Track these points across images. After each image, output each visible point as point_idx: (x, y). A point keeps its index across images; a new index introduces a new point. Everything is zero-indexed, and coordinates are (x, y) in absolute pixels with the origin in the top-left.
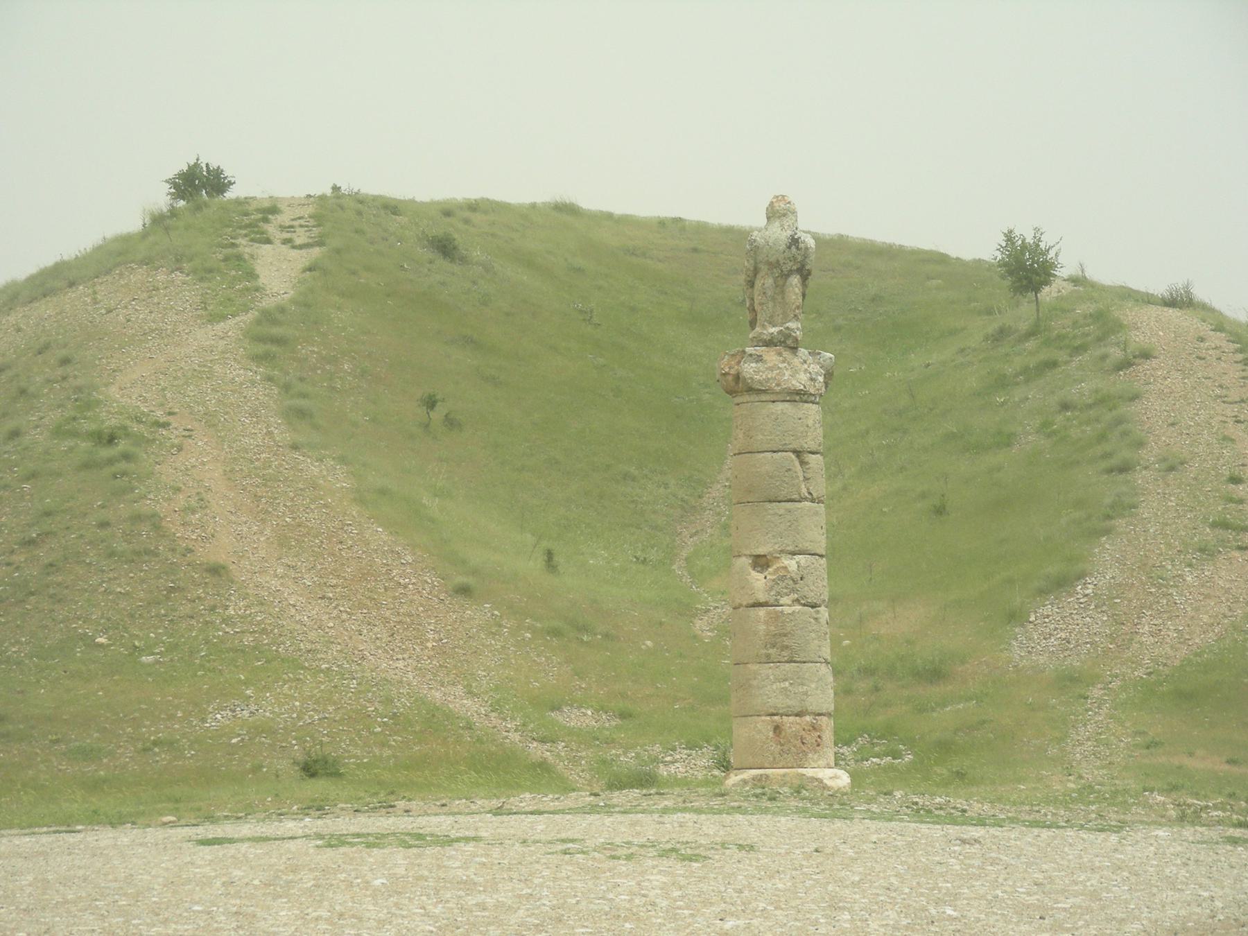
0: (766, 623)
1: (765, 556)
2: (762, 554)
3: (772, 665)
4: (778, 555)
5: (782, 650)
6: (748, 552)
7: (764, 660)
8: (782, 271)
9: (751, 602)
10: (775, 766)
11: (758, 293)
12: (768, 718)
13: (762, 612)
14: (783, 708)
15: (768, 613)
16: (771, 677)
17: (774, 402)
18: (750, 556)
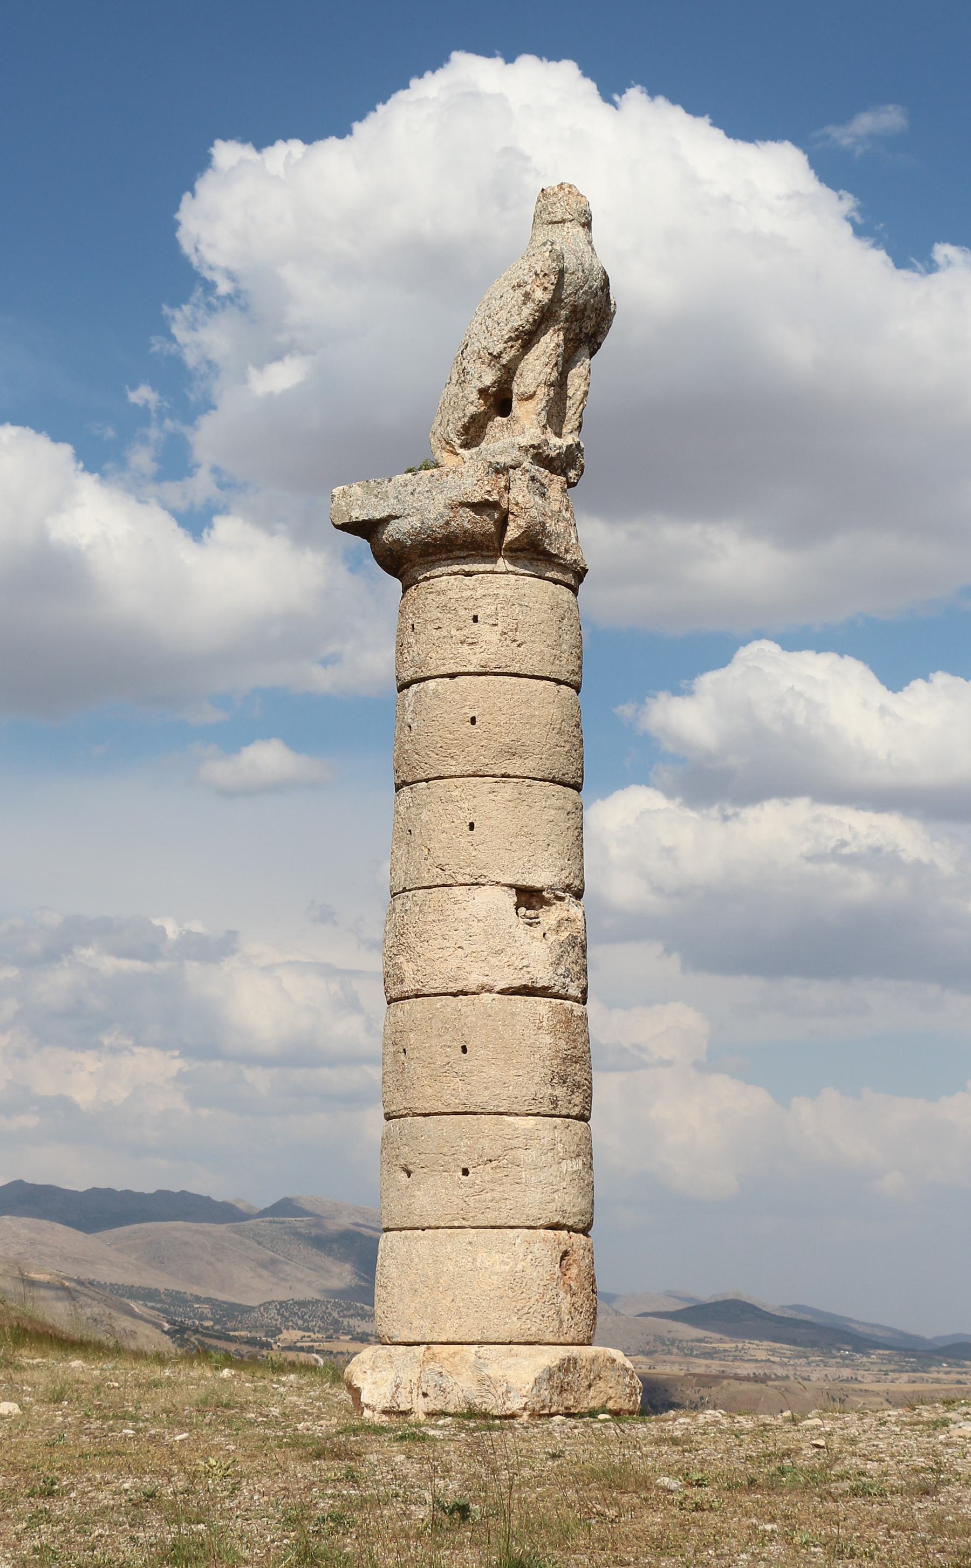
0: (553, 1032)
1: (540, 891)
2: (539, 885)
3: (559, 1120)
4: (563, 895)
5: (573, 1092)
6: (510, 880)
7: (545, 1109)
8: (581, 331)
9: (516, 983)
10: (562, 1340)
11: (544, 359)
12: (551, 1233)
13: (542, 1005)
14: (575, 1214)
15: (554, 1011)
16: (559, 1147)
17: (556, 582)
18: (511, 886)
